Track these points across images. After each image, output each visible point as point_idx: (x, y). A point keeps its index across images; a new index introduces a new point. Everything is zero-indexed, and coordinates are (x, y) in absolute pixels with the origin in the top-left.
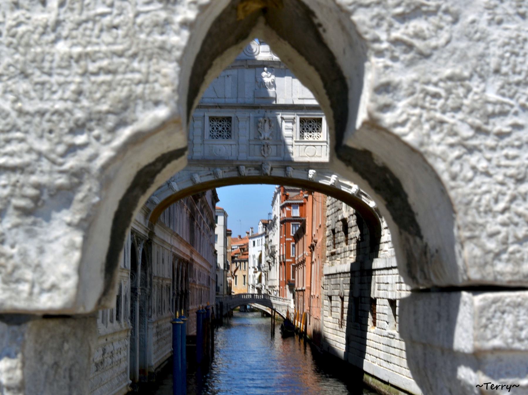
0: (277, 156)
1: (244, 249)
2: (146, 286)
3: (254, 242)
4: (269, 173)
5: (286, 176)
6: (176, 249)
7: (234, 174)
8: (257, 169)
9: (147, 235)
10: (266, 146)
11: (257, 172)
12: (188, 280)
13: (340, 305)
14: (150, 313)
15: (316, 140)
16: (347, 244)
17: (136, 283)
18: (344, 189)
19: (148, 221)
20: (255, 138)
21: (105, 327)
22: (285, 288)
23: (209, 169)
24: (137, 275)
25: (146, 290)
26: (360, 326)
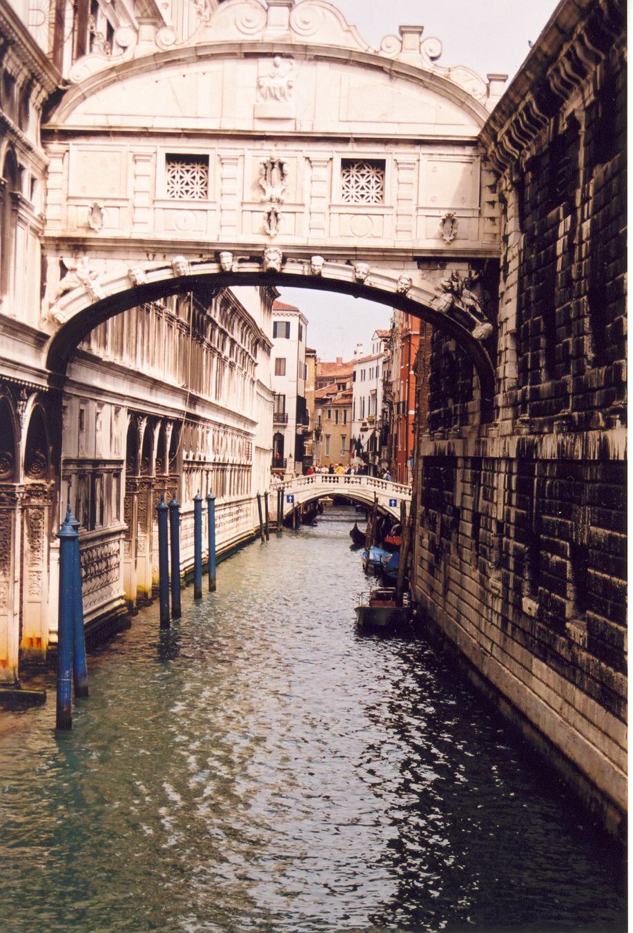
1: (344, 385)
3: (363, 372)
4: (278, 269)
5: (310, 274)
7: (212, 269)
9: (44, 383)
11: (258, 265)
12: (180, 455)
15: (372, 203)
16: (455, 402)
18: (423, 300)
19: (44, 356)
20: (253, 199)
22: (406, 466)
23: (164, 257)
26: (461, 564)
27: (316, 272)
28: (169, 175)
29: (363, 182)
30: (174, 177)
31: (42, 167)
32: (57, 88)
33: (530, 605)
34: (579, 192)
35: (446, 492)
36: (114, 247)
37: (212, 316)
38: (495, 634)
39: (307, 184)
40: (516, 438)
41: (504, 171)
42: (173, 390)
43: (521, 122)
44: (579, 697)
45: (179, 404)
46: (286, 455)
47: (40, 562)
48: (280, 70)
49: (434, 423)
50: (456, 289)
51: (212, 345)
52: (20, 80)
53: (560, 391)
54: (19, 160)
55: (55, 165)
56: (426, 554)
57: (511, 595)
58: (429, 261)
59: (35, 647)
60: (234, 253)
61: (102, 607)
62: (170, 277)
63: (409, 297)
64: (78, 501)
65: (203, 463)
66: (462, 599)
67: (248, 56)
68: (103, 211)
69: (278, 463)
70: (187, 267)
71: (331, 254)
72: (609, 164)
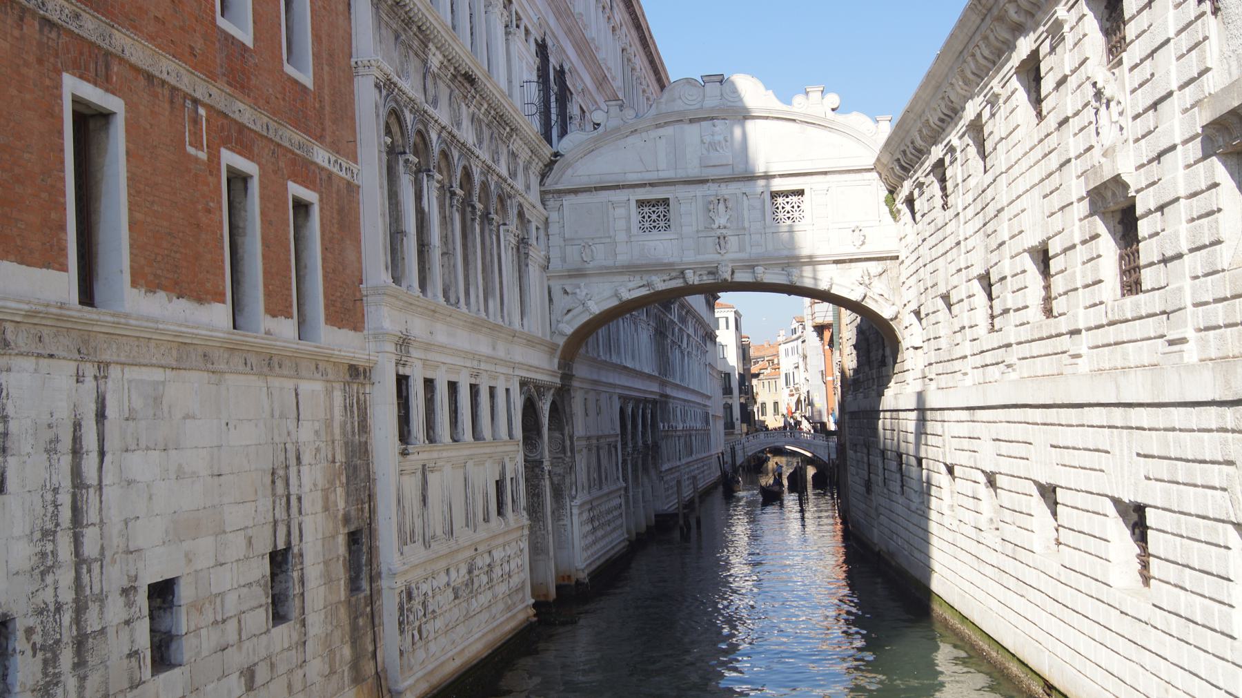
0: (740, 251)
2: (564, 452)
4: (729, 280)
7: (678, 283)
8: (710, 273)
9: (558, 381)
10: (722, 238)
11: (711, 277)
13: (866, 459)
14: (574, 492)
17: (542, 453)
19: (556, 361)
20: (705, 228)
21: (471, 532)
23: (641, 277)
24: (543, 443)
25: (564, 460)
27: (759, 279)
28: (640, 217)
29: (788, 208)
30: (644, 217)
31: (544, 219)
32: (551, 160)
35: (872, 439)
37: (672, 318)
39: (746, 213)
41: (896, 189)
42: (650, 377)
43: (908, 153)
46: (734, 420)
47: (565, 518)
48: (717, 129)
50: (867, 282)
51: (673, 339)
54: (527, 216)
55: (554, 216)
59: (566, 582)
60: (694, 273)
61: (613, 548)
62: (648, 292)
63: (832, 291)
64: (589, 468)
65: (676, 431)
66: (892, 520)
67: (691, 121)
68: (593, 247)
69: (730, 425)
70: (660, 284)
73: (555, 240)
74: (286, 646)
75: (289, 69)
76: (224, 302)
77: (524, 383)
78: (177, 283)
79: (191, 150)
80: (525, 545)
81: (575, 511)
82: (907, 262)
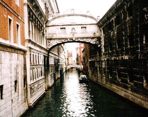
6: (55, 57)
7: (67, 41)
29: (84, 30)
33: (110, 77)
34: (114, 29)
36: (55, 39)
38: (104, 81)
40: (106, 58)
44: (120, 88)
45: (58, 57)
49: (90, 58)
52: (43, 20)
53: (113, 53)
55: (47, 30)
56: (91, 73)
57: (107, 77)
58: (93, 38)
70: (63, 41)
71: (81, 38)
72: (119, 25)
73: (47, 34)
74: (17, 96)
75: (16, 3)
76: (8, 40)
77: (44, 56)
78: (3, 37)
79: (4, 15)
80: (44, 81)
81: (49, 76)
82: (102, 38)
